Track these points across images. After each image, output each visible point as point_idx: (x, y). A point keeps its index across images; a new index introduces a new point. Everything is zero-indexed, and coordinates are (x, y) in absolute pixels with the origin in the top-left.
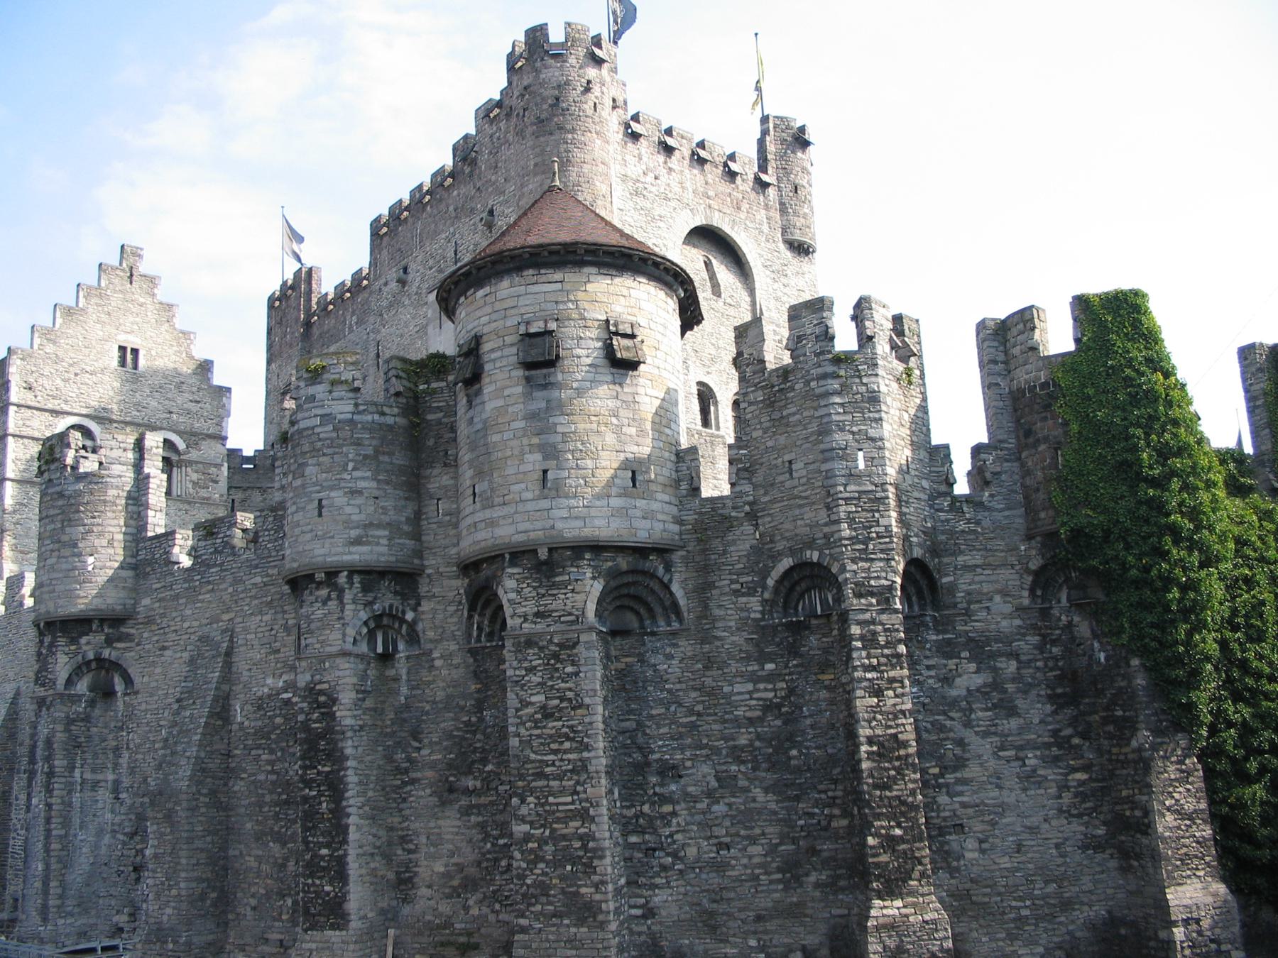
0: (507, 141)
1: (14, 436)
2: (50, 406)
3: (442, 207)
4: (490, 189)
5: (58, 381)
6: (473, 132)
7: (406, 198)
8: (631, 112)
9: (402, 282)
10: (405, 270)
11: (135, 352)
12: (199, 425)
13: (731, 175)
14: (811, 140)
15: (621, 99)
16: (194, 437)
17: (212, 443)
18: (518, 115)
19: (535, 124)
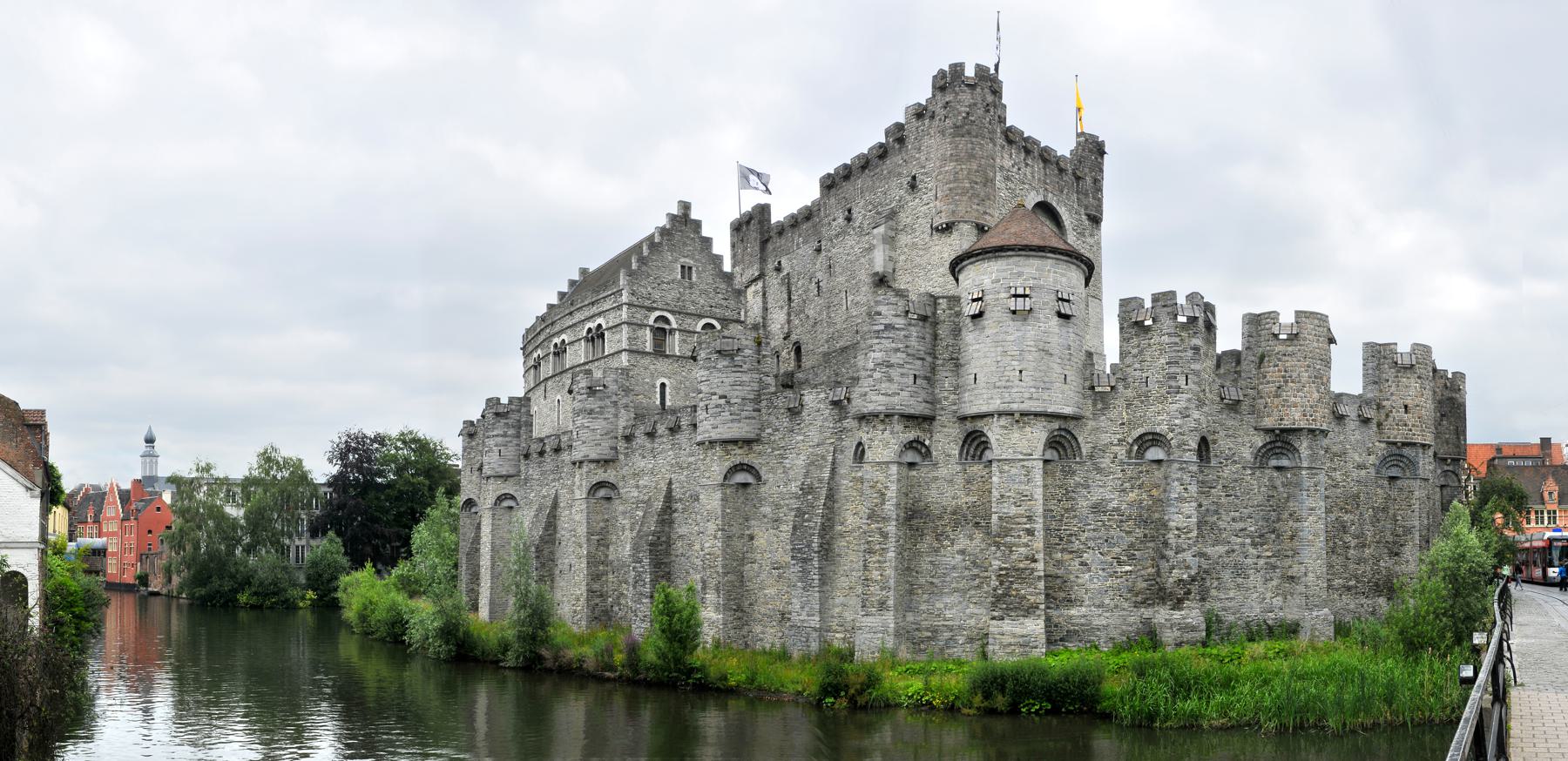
1: (627, 323)
9: (849, 219)
10: (849, 211)
11: (690, 268)
12: (728, 314)
16: (725, 321)
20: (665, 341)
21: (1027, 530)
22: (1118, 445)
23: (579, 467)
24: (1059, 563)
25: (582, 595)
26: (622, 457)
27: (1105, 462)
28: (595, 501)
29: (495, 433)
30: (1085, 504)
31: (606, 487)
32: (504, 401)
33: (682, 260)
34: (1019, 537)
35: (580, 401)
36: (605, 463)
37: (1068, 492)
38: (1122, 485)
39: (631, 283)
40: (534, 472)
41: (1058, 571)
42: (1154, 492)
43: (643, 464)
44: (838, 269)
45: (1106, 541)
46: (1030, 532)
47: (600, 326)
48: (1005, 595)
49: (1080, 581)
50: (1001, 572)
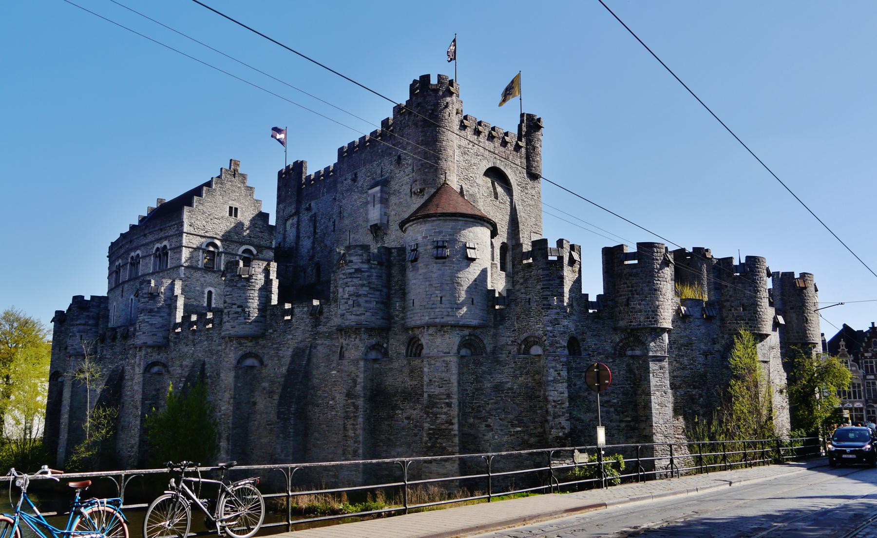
0: (408, 125)
1: (185, 247)
2: (200, 234)
3: (375, 149)
5: (204, 222)
7: (357, 140)
8: (464, 114)
10: (356, 174)
11: (236, 209)
13: (504, 144)
14: (542, 126)
15: (460, 109)
17: (268, 251)
19: (421, 121)
20: (214, 260)
21: (447, 403)
22: (512, 345)
23: (140, 351)
24: (472, 426)
25: (135, 443)
26: (172, 344)
27: (503, 357)
28: (150, 376)
29: (78, 322)
30: (489, 386)
31: (158, 365)
32: (87, 298)
33: (230, 202)
34: (442, 408)
35: (142, 303)
36: (159, 347)
38: (514, 372)
39: (190, 217)
40: (108, 354)
42: (537, 377)
43: (186, 350)
44: (345, 214)
45: (504, 410)
46: (449, 405)
47: (165, 246)
48: (432, 447)
49: (486, 438)
50: (430, 432)
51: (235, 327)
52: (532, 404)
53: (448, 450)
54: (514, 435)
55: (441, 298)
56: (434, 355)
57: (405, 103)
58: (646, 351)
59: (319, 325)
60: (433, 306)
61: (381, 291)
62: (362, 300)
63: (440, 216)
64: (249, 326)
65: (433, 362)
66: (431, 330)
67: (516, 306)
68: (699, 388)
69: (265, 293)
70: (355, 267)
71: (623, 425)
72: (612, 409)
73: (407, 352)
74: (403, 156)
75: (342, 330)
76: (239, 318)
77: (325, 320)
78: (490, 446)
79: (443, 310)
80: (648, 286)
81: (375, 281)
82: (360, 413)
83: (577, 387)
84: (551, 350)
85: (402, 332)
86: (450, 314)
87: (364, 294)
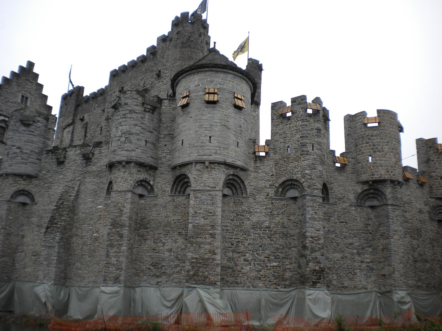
4: (160, 64)
6: (156, 45)
11: (27, 98)
18: (175, 40)
19: (180, 44)
21: (211, 234)
22: (270, 188)
24: (230, 259)
37: (238, 215)
38: (272, 212)
41: (230, 264)
42: (291, 218)
45: (261, 246)
46: (213, 236)
48: (194, 275)
49: (243, 271)
51: (12, 166)
52: (287, 242)
53: (210, 279)
54: (270, 269)
55: (210, 137)
56: (201, 189)
57: (167, 34)
58: (384, 200)
59: (90, 165)
60: (202, 144)
61: (152, 132)
62: (134, 139)
63: (213, 67)
64: (24, 165)
65: (199, 195)
66: (199, 166)
67: (275, 154)
68: (417, 239)
69: (43, 140)
70: (131, 109)
71: (364, 265)
72: (355, 251)
73: (172, 191)
74: (162, 71)
75: (111, 166)
76: (17, 158)
77: (95, 161)
78: (247, 279)
79: (211, 148)
80: (387, 145)
81: (148, 123)
82: (124, 242)
83: (326, 229)
84: (309, 191)
85: (169, 172)
86: (218, 152)
87: (135, 133)
